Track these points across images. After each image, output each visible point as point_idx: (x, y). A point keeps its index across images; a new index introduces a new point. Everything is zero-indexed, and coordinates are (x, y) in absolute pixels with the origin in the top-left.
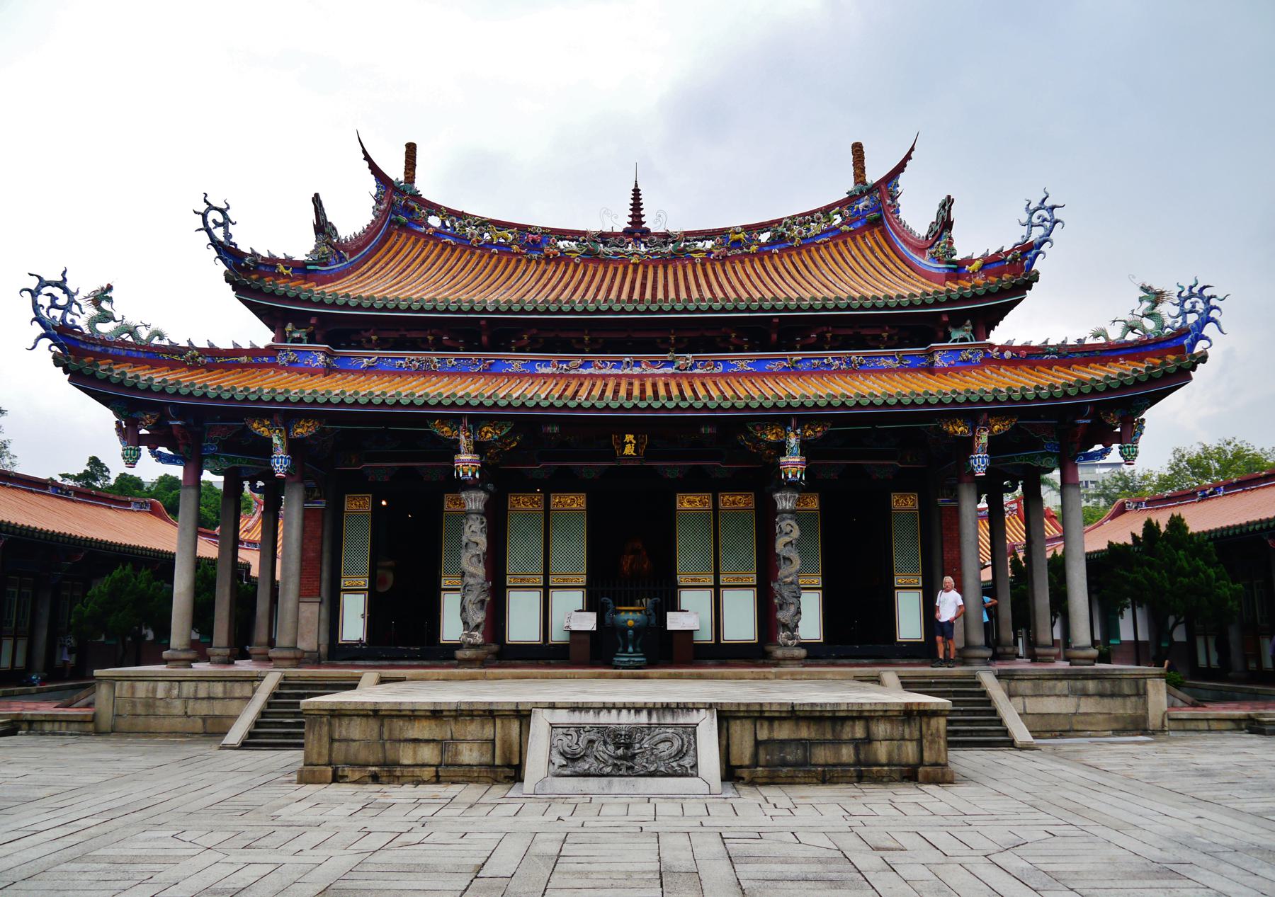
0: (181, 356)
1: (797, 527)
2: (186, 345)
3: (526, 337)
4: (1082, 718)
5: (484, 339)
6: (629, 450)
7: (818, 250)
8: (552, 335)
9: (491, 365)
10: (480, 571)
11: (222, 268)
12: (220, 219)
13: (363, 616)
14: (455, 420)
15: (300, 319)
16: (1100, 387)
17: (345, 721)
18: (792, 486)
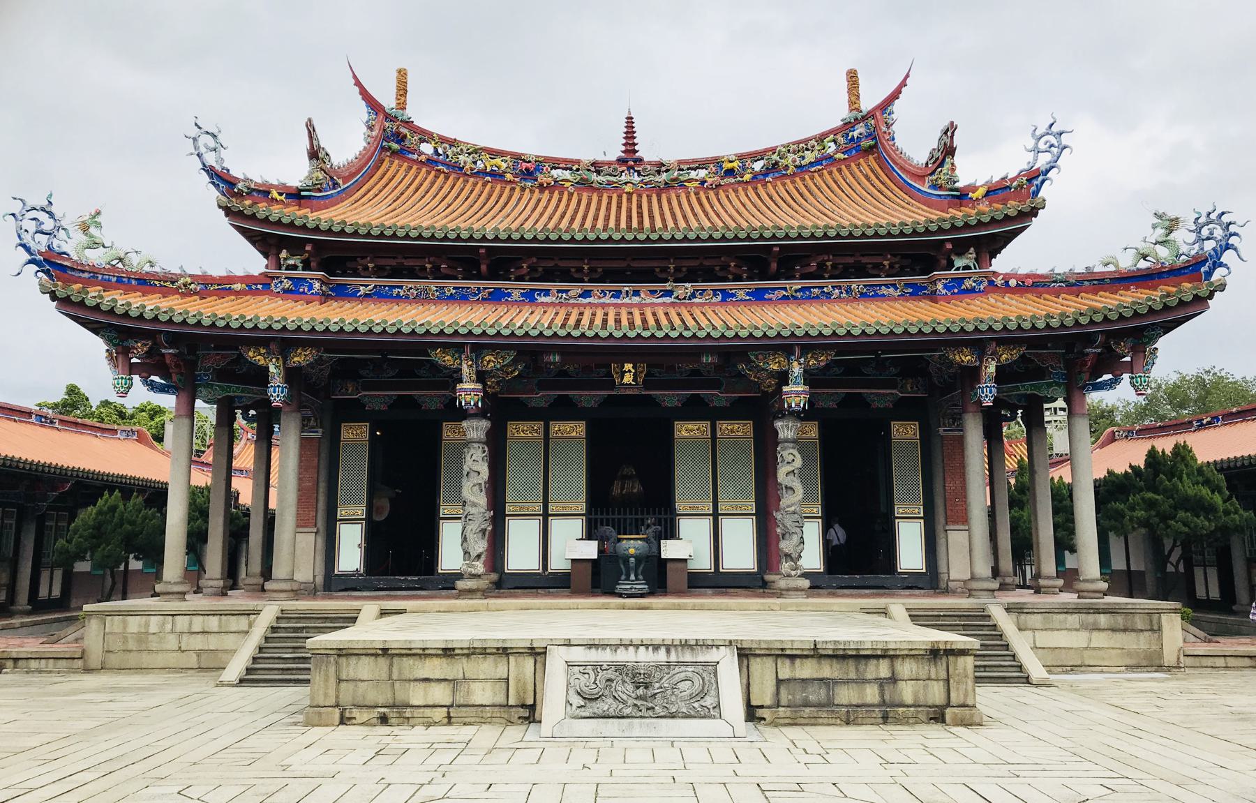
0: (173, 283)
1: (798, 456)
2: (178, 272)
3: (525, 266)
4: (1094, 653)
5: (484, 268)
6: (628, 379)
7: (812, 178)
8: (551, 264)
9: (490, 294)
10: (482, 500)
11: (213, 194)
12: (212, 144)
14: (459, 348)
15: (295, 246)
16: (1113, 316)
17: (353, 660)
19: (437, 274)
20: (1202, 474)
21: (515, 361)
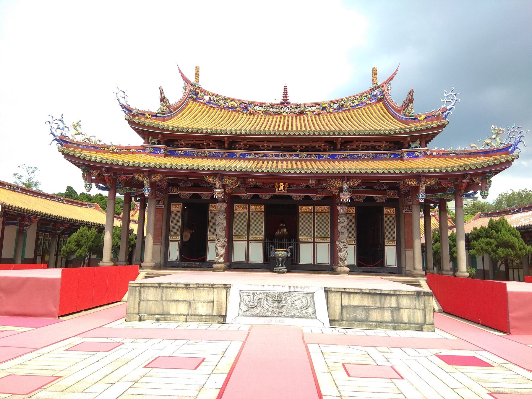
2: (110, 144)
5: (226, 145)
6: (281, 189)
7: (357, 111)
9: (228, 155)
10: (223, 234)
12: (124, 96)
13: (177, 250)
14: (216, 175)
18: (345, 204)
19: (208, 147)
20: (510, 230)
21: (237, 181)
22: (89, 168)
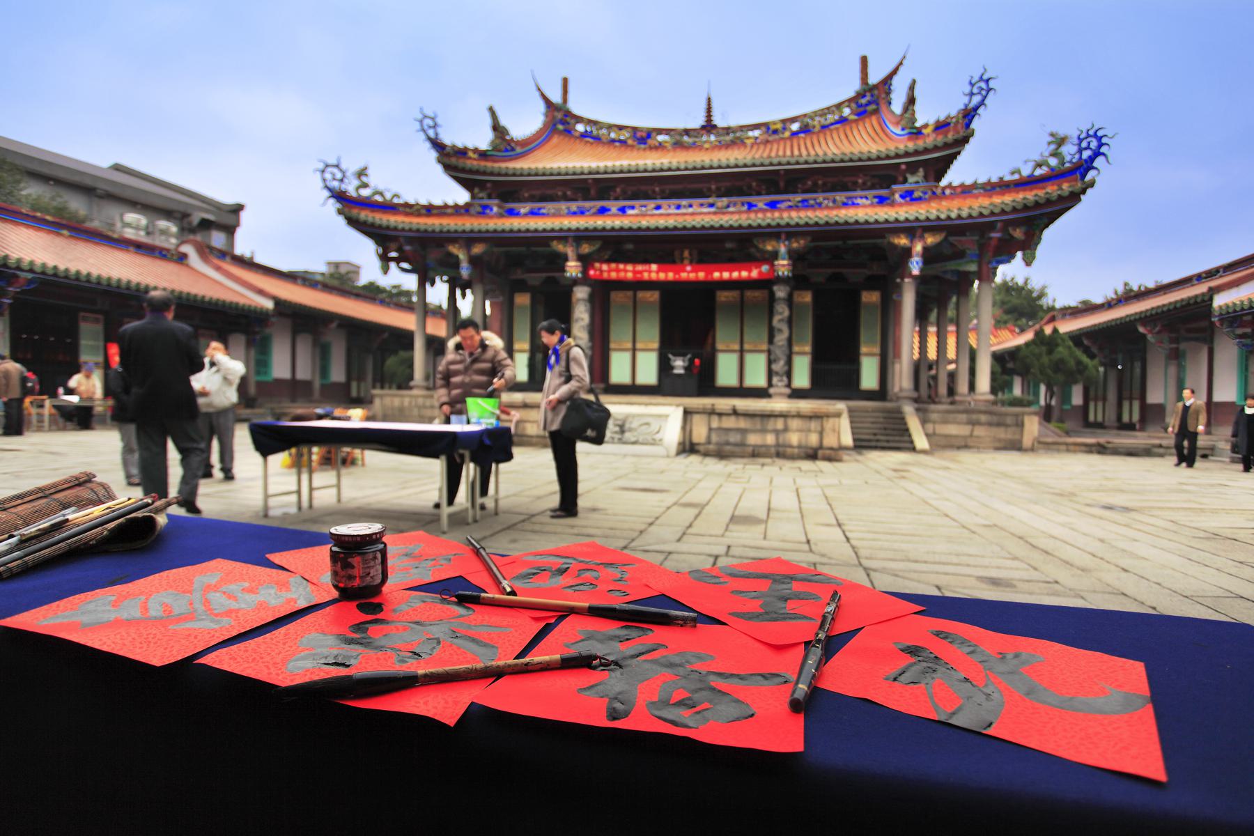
11: (433, 154)
15: (481, 185)
19: (566, 199)
22: (384, 239)
